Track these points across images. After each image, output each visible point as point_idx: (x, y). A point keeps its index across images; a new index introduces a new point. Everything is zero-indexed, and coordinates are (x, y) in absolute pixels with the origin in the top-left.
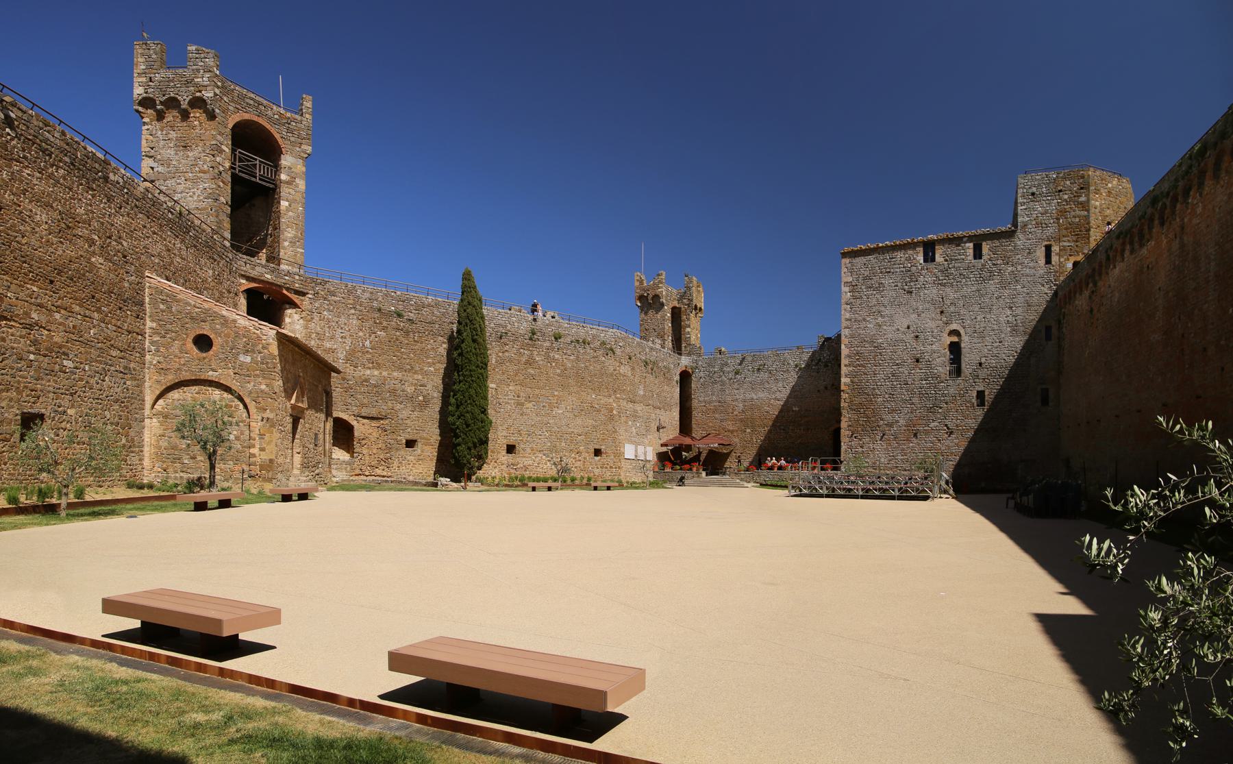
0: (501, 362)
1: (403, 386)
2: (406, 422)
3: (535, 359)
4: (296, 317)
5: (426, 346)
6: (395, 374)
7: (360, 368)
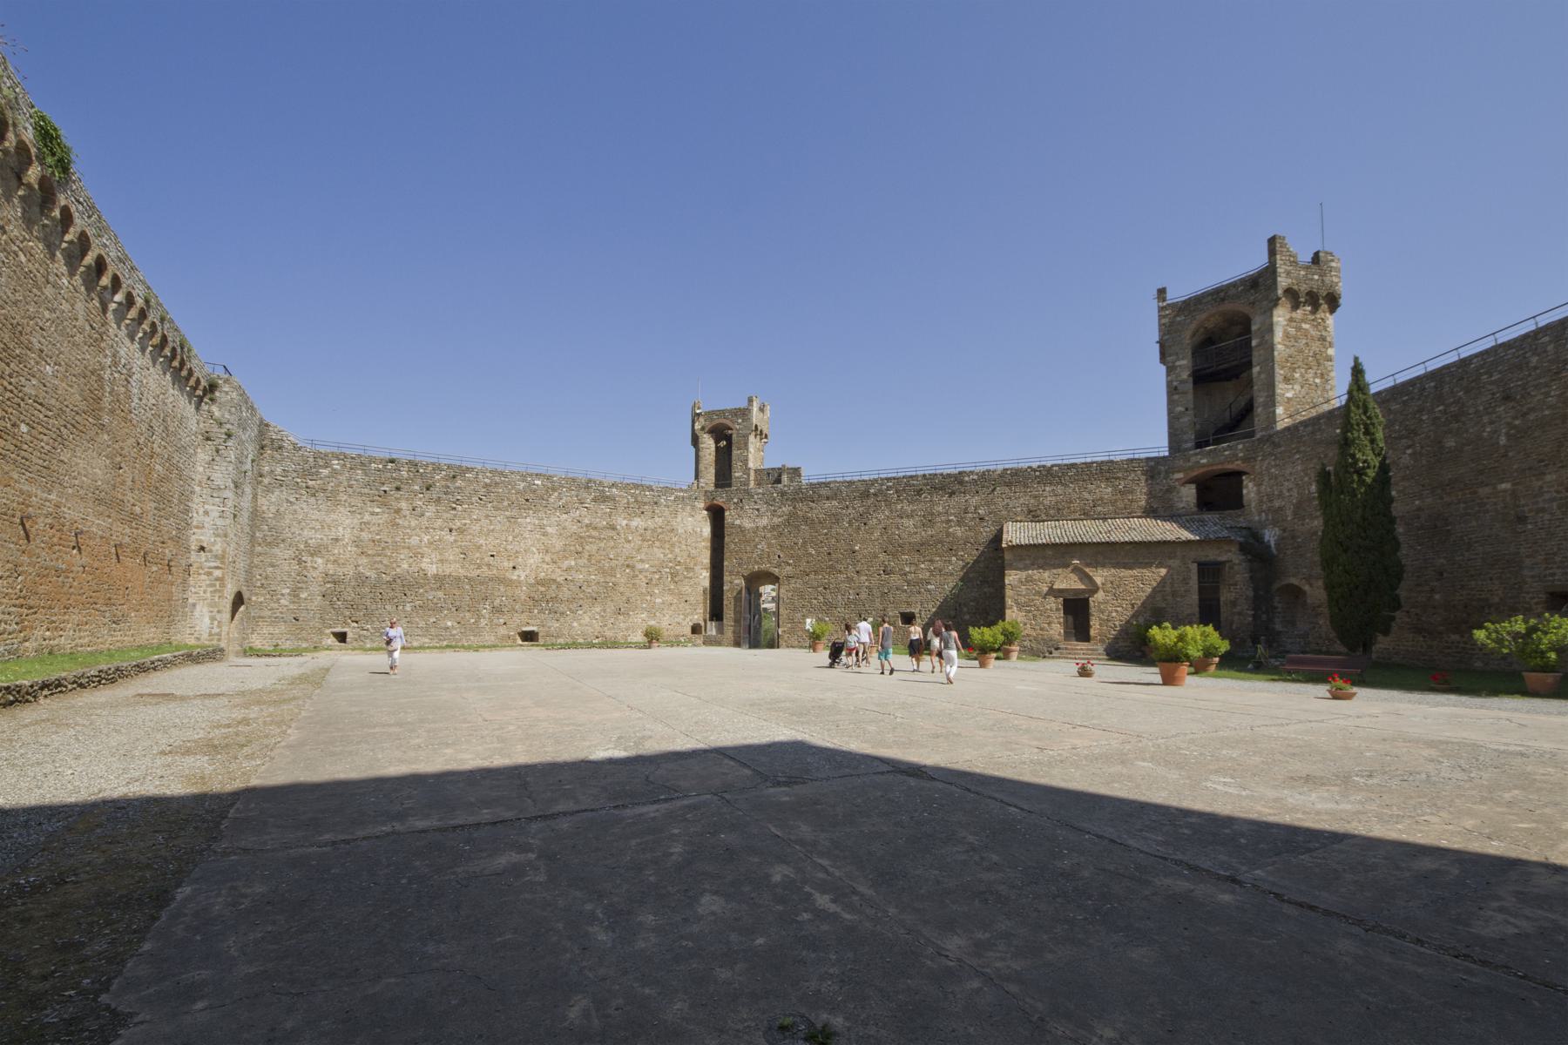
4: (1251, 485)
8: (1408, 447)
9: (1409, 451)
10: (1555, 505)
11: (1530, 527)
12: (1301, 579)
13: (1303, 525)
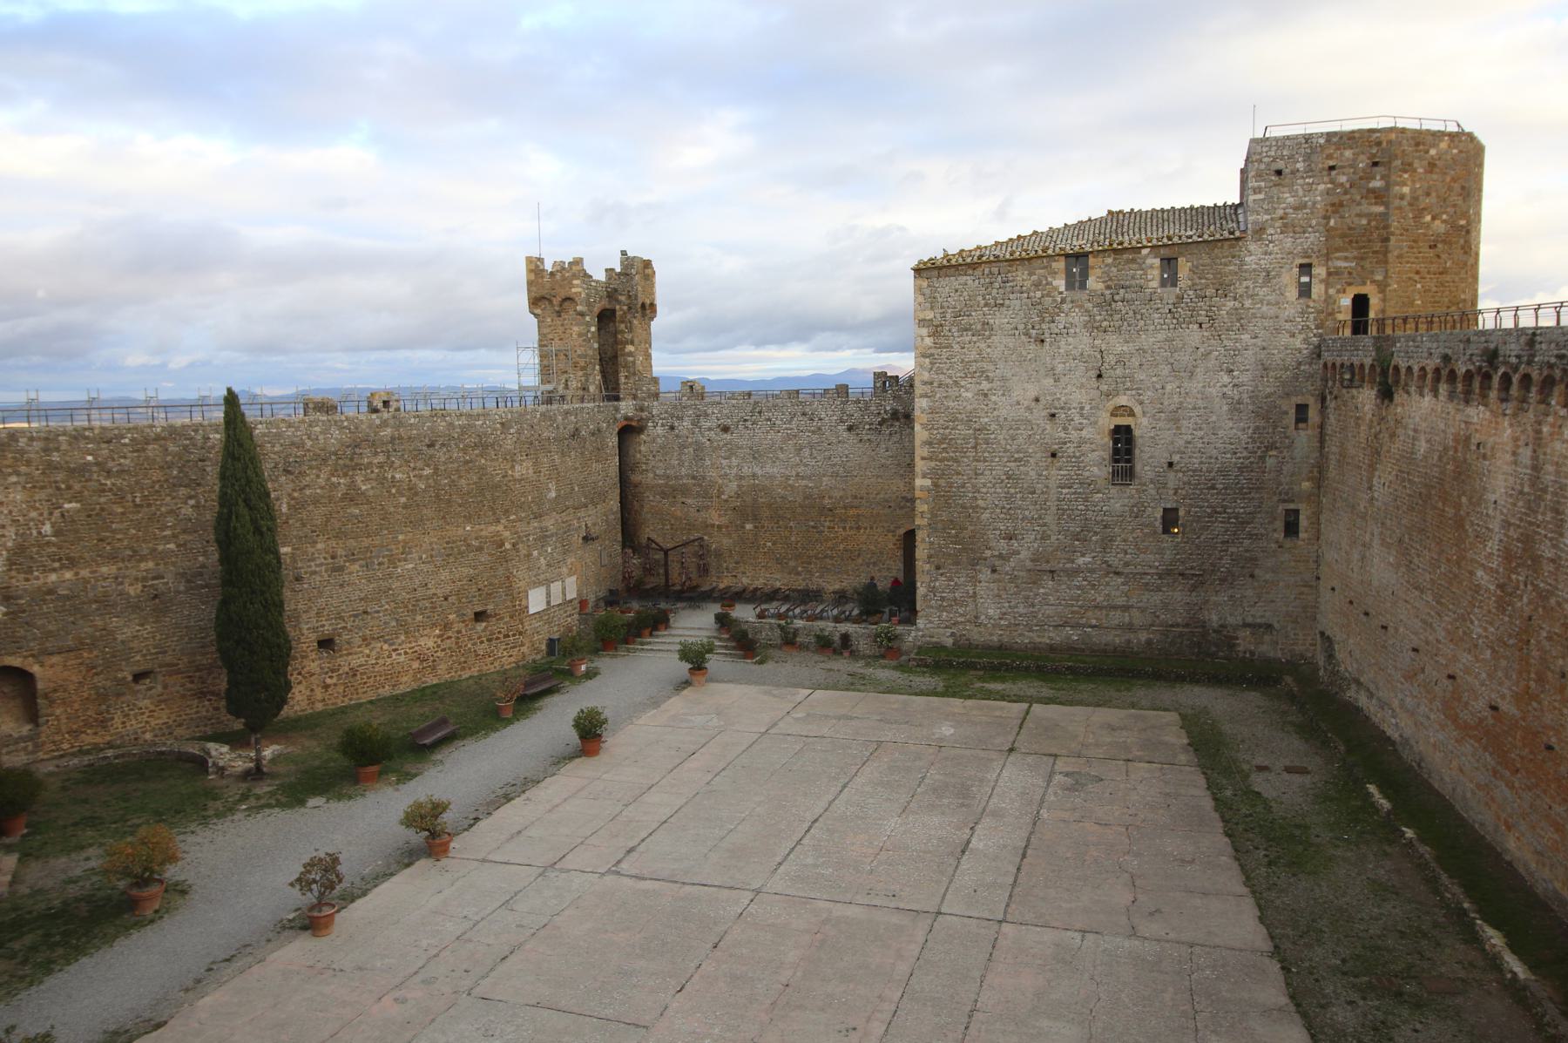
0: (297, 506)
1: (120, 587)
2: (131, 645)
3: (360, 489)
5: (159, 510)
6: (104, 570)
7: (36, 573)
8: (191, 497)
9: (192, 502)
10: (323, 568)
11: (305, 586)
12: (25, 657)
13: (27, 580)
